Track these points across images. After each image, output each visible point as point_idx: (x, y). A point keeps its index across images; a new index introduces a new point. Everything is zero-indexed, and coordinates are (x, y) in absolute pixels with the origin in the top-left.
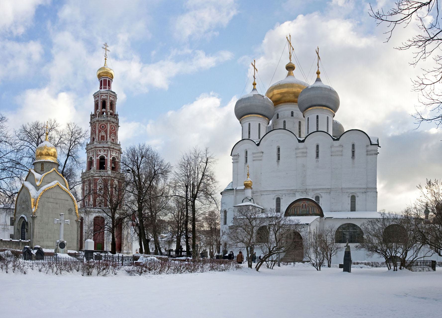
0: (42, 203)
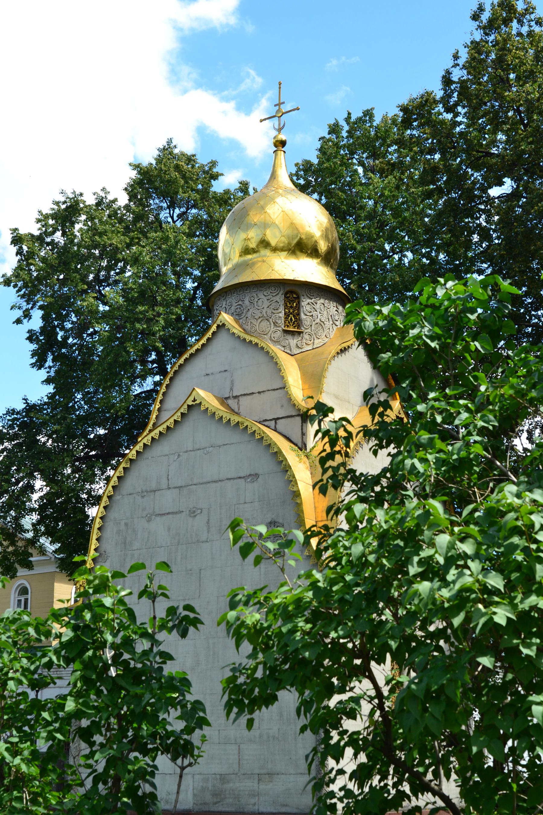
0: (123, 527)
